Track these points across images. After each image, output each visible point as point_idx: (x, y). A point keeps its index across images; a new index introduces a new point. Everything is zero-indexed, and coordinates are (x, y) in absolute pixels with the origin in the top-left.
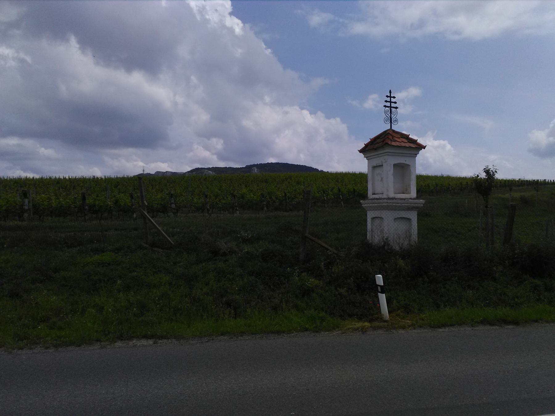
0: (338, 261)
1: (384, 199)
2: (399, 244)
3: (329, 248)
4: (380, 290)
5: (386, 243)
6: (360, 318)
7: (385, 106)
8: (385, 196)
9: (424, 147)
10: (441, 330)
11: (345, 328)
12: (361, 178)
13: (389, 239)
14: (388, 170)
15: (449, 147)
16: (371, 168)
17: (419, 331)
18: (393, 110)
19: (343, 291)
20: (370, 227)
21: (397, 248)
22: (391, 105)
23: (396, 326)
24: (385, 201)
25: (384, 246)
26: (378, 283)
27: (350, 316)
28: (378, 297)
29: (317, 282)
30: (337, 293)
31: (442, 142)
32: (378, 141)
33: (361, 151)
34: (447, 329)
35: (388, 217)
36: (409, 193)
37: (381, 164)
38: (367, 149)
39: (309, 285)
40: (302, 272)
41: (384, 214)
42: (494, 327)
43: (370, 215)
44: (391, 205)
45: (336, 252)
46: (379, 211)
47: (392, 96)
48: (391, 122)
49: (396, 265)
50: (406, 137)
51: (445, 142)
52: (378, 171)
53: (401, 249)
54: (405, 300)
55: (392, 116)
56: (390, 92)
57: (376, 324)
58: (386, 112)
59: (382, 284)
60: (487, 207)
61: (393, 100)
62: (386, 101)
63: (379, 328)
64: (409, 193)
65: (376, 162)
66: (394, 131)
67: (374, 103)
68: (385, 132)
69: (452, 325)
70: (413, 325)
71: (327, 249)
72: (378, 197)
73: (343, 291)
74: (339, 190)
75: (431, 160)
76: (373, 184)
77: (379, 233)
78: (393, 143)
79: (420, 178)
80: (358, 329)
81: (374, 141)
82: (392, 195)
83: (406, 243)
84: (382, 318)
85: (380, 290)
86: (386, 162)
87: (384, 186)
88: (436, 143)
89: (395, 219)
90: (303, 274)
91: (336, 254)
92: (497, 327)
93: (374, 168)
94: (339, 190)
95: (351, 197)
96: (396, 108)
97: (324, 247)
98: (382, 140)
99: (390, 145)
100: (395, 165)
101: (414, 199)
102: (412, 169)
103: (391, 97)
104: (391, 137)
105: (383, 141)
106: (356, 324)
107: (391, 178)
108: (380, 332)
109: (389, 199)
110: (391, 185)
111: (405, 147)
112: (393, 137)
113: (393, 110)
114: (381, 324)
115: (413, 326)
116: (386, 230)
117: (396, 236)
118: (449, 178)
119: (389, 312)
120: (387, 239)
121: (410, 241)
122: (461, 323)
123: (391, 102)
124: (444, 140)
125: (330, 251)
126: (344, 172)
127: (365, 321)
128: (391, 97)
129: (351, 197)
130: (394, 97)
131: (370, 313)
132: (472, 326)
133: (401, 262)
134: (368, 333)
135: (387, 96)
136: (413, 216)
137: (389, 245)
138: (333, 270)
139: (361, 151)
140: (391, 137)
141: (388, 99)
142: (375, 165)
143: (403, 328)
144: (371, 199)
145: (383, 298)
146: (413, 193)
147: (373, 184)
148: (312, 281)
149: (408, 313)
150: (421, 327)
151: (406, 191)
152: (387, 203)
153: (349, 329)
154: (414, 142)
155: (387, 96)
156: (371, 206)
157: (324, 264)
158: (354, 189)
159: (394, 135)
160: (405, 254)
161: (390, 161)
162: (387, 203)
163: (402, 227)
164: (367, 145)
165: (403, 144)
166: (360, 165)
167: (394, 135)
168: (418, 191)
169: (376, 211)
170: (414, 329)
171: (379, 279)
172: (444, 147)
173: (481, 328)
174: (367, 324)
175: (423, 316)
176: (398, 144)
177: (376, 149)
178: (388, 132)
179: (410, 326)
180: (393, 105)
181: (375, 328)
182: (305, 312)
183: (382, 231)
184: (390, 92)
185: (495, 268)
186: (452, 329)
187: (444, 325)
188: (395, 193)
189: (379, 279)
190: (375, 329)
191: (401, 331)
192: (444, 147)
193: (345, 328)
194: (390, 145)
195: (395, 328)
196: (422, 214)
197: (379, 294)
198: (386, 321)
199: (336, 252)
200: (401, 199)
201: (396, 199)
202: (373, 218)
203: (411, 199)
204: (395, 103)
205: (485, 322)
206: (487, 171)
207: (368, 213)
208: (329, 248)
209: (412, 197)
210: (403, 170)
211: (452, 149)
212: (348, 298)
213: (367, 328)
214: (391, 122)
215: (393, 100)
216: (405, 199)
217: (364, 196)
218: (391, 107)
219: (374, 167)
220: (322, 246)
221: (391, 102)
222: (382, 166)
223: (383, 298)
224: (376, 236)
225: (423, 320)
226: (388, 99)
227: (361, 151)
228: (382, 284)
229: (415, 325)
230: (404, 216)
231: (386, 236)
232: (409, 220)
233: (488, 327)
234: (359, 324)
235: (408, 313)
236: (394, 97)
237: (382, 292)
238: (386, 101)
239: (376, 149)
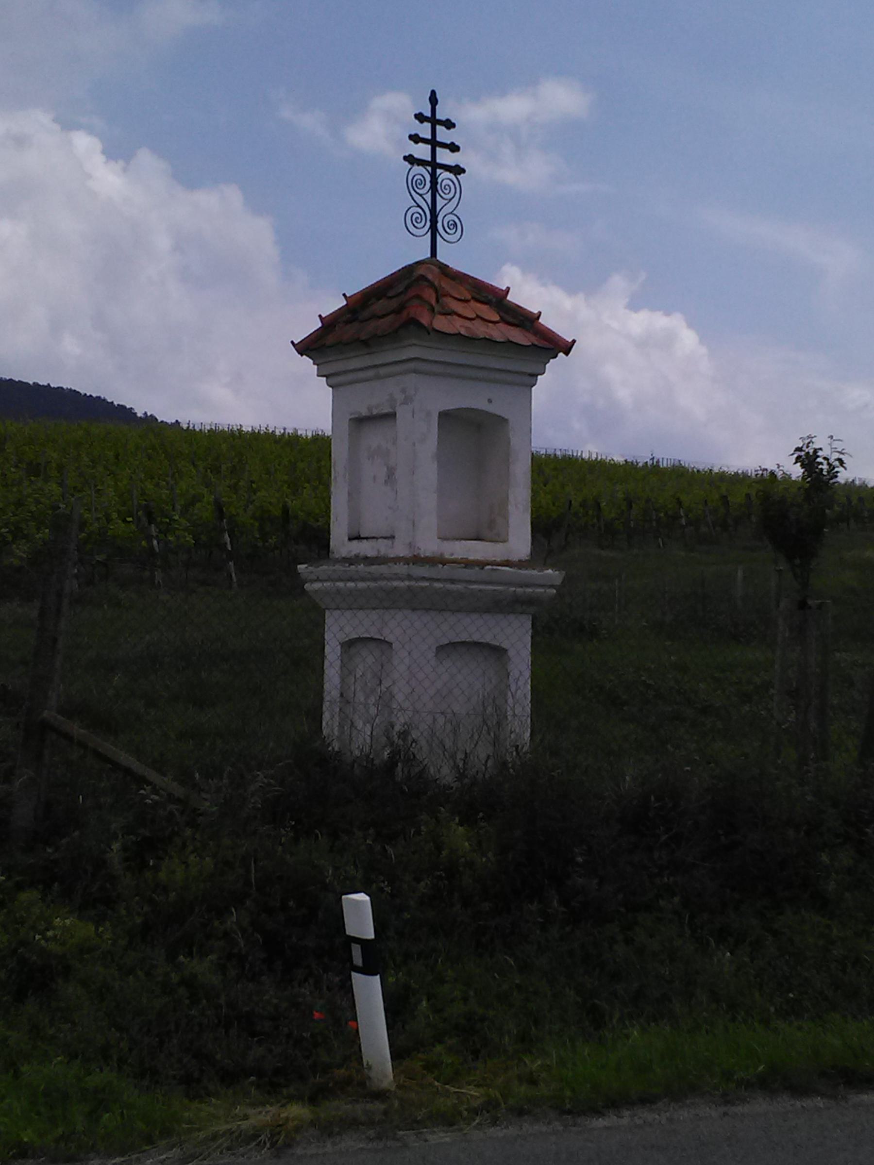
0: (188, 832)
1: (397, 560)
2: (453, 756)
3: (152, 775)
4: (358, 960)
5: (401, 751)
6: (274, 1084)
7: (410, 159)
8: (400, 550)
9: (567, 348)
10: (600, 1123)
11: (202, 1135)
12: (300, 459)
13: (414, 734)
14: (418, 438)
15: (688, 339)
16: (346, 425)
17: (512, 1131)
18: (444, 176)
19: (202, 968)
20: (337, 680)
21: (446, 774)
22: (433, 158)
23: (420, 1115)
24: (401, 569)
25: (392, 763)
26: (351, 930)
27: (230, 1078)
28: (347, 989)
29: (85, 930)
30: (175, 978)
31: (660, 321)
32: (380, 306)
33: (305, 348)
34: (626, 1118)
35: (413, 637)
36: (500, 538)
37: (386, 410)
38: (330, 340)
39: (53, 947)
40: (20, 887)
41: (396, 626)
42: (808, 1103)
43: (338, 628)
44: (427, 587)
45: (178, 791)
46: (374, 615)
47: (428, 126)
48: (434, 229)
49: (439, 848)
50: (496, 299)
51: (676, 323)
52: (374, 438)
53: (461, 776)
54: (465, 999)
55: (440, 202)
56: (433, 100)
57: (338, 1107)
58: (413, 185)
59: (370, 934)
60: (803, 605)
61: (443, 135)
62: (415, 138)
63: (351, 1124)
64: (500, 538)
65: (369, 397)
66: (444, 269)
67: (382, 130)
68: (408, 270)
69: (647, 1100)
70: (490, 1105)
71: (142, 781)
72: (371, 553)
73: (202, 968)
74: (219, 509)
75: (623, 394)
76: (354, 494)
77: (373, 711)
78: (441, 323)
79: (552, 470)
80: (255, 1136)
81: (359, 307)
82: (429, 546)
83: (483, 751)
84: (362, 1084)
85: (358, 960)
86: (407, 400)
87: (398, 504)
88: (640, 322)
89: (441, 649)
90: (25, 896)
91: (179, 801)
92: (819, 1102)
93: (361, 422)
94: (219, 509)
95: (272, 541)
96: (458, 170)
97: (128, 771)
98: (394, 304)
99: (426, 325)
100: (445, 416)
101: (520, 564)
102: (515, 440)
103: (434, 121)
104: (430, 295)
105: (398, 311)
106: (250, 1111)
107: (428, 472)
108: (350, 1142)
109: (417, 560)
110: (429, 501)
111: (489, 342)
112: (440, 295)
113: (444, 176)
114: (359, 1109)
115: (490, 1111)
116: (400, 697)
117: (441, 720)
118: (680, 475)
119: (397, 1054)
120: (404, 734)
121: (496, 742)
122: (680, 1090)
123: (434, 143)
124: (668, 314)
125: (155, 791)
126: (247, 428)
127: (291, 1098)
128: (434, 121)
129: (272, 541)
130: (449, 125)
131: (317, 1063)
132: (727, 1100)
133: (459, 837)
134: (299, 1151)
135: (420, 117)
136: (516, 636)
137: (411, 759)
138: (162, 875)
139: (305, 348)
140: (430, 295)
141: (425, 131)
142: (364, 412)
143: (448, 1120)
144: (351, 561)
145: (369, 992)
146: (519, 541)
147: (354, 494)
148: (68, 928)
149: (476, 1054)
150: (520, 1112)
151: (488, 529)
152: (409, 577)
153: (214, 1137)
154: (527, 320)
155: (420, 117)
156: (339, 591)
157: (125, 849)
158: (285, 510)
159: (446, 285)
160: (477, 800)
161: (424, 399)
162: (409, 577)
163: (469, 681)
164: (329, 324)
165: (481, 330)
166: (301, 403)
167: (446, 285)
168: (542, 528)
169: (361, 614)
170: (495, 1122)
171: (359, 912)
172: (667, 342)
173: (761, 1105)
174: (297, 1111)
175: (534, 1064)
176: (458, 326)
177: (366, 343)
178: (421, 271)
179: (476, 1112)
180: (444, 157)
181: (328, 1129)
182: (24, 1069)
183: (385, 701)
184: (433, 100)
185: (825, 858)
186: (645, 1115)
187: (615, 1103)
188: (444, 539)
189: (359, 912)
190: (330, 1135)
191: (440, 1137)
192: (667, 342)
193: (202, 1135)
194: (426, 325)
195: (415, 1125)
196: (555, 629)
197: (356, 977)
198: (380, 1095)
199: (178, 791)
200: (468, 564)
201: (444, 562)
202: (349, 645)
203: (507, 563)
204: (454, 148)
205: (778, 1081)
206: (808, 459)
207: (330, 619)
208: (152, 775)
209: (515, 558)
210: (475, 435)
211: (703, 350)
212: (222, 1000)
213: (297, 1129)
214: (434, 229)
215: (443, 135)
216: (482, 564)
217: (317, 541)
218: (434, 165)
219: (360, 422)
220: (117, 766)
221: (434, 143)
222: (392, 416)
223: (369, 992)
224: (359, 724)
225: (533, 1082)
226: (425, 131)
227: (307, 347)
228: (370, 934)
229: (497, 1106)
230: (476, 638)
231: (400, 721)
232: (498, 652)
233: (785, 1103)
234: (261, 1116)
235: (476, 1054)
236: (449, 125)
237: (367, 970)
238: (415, 138)
239: (367, 344)
